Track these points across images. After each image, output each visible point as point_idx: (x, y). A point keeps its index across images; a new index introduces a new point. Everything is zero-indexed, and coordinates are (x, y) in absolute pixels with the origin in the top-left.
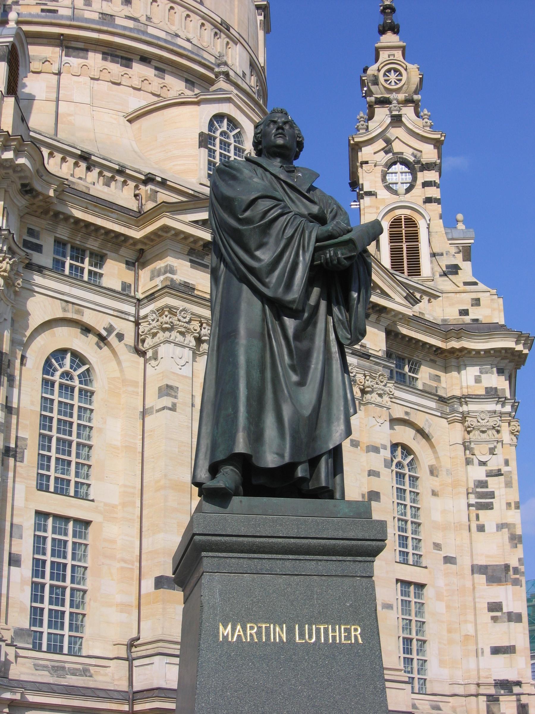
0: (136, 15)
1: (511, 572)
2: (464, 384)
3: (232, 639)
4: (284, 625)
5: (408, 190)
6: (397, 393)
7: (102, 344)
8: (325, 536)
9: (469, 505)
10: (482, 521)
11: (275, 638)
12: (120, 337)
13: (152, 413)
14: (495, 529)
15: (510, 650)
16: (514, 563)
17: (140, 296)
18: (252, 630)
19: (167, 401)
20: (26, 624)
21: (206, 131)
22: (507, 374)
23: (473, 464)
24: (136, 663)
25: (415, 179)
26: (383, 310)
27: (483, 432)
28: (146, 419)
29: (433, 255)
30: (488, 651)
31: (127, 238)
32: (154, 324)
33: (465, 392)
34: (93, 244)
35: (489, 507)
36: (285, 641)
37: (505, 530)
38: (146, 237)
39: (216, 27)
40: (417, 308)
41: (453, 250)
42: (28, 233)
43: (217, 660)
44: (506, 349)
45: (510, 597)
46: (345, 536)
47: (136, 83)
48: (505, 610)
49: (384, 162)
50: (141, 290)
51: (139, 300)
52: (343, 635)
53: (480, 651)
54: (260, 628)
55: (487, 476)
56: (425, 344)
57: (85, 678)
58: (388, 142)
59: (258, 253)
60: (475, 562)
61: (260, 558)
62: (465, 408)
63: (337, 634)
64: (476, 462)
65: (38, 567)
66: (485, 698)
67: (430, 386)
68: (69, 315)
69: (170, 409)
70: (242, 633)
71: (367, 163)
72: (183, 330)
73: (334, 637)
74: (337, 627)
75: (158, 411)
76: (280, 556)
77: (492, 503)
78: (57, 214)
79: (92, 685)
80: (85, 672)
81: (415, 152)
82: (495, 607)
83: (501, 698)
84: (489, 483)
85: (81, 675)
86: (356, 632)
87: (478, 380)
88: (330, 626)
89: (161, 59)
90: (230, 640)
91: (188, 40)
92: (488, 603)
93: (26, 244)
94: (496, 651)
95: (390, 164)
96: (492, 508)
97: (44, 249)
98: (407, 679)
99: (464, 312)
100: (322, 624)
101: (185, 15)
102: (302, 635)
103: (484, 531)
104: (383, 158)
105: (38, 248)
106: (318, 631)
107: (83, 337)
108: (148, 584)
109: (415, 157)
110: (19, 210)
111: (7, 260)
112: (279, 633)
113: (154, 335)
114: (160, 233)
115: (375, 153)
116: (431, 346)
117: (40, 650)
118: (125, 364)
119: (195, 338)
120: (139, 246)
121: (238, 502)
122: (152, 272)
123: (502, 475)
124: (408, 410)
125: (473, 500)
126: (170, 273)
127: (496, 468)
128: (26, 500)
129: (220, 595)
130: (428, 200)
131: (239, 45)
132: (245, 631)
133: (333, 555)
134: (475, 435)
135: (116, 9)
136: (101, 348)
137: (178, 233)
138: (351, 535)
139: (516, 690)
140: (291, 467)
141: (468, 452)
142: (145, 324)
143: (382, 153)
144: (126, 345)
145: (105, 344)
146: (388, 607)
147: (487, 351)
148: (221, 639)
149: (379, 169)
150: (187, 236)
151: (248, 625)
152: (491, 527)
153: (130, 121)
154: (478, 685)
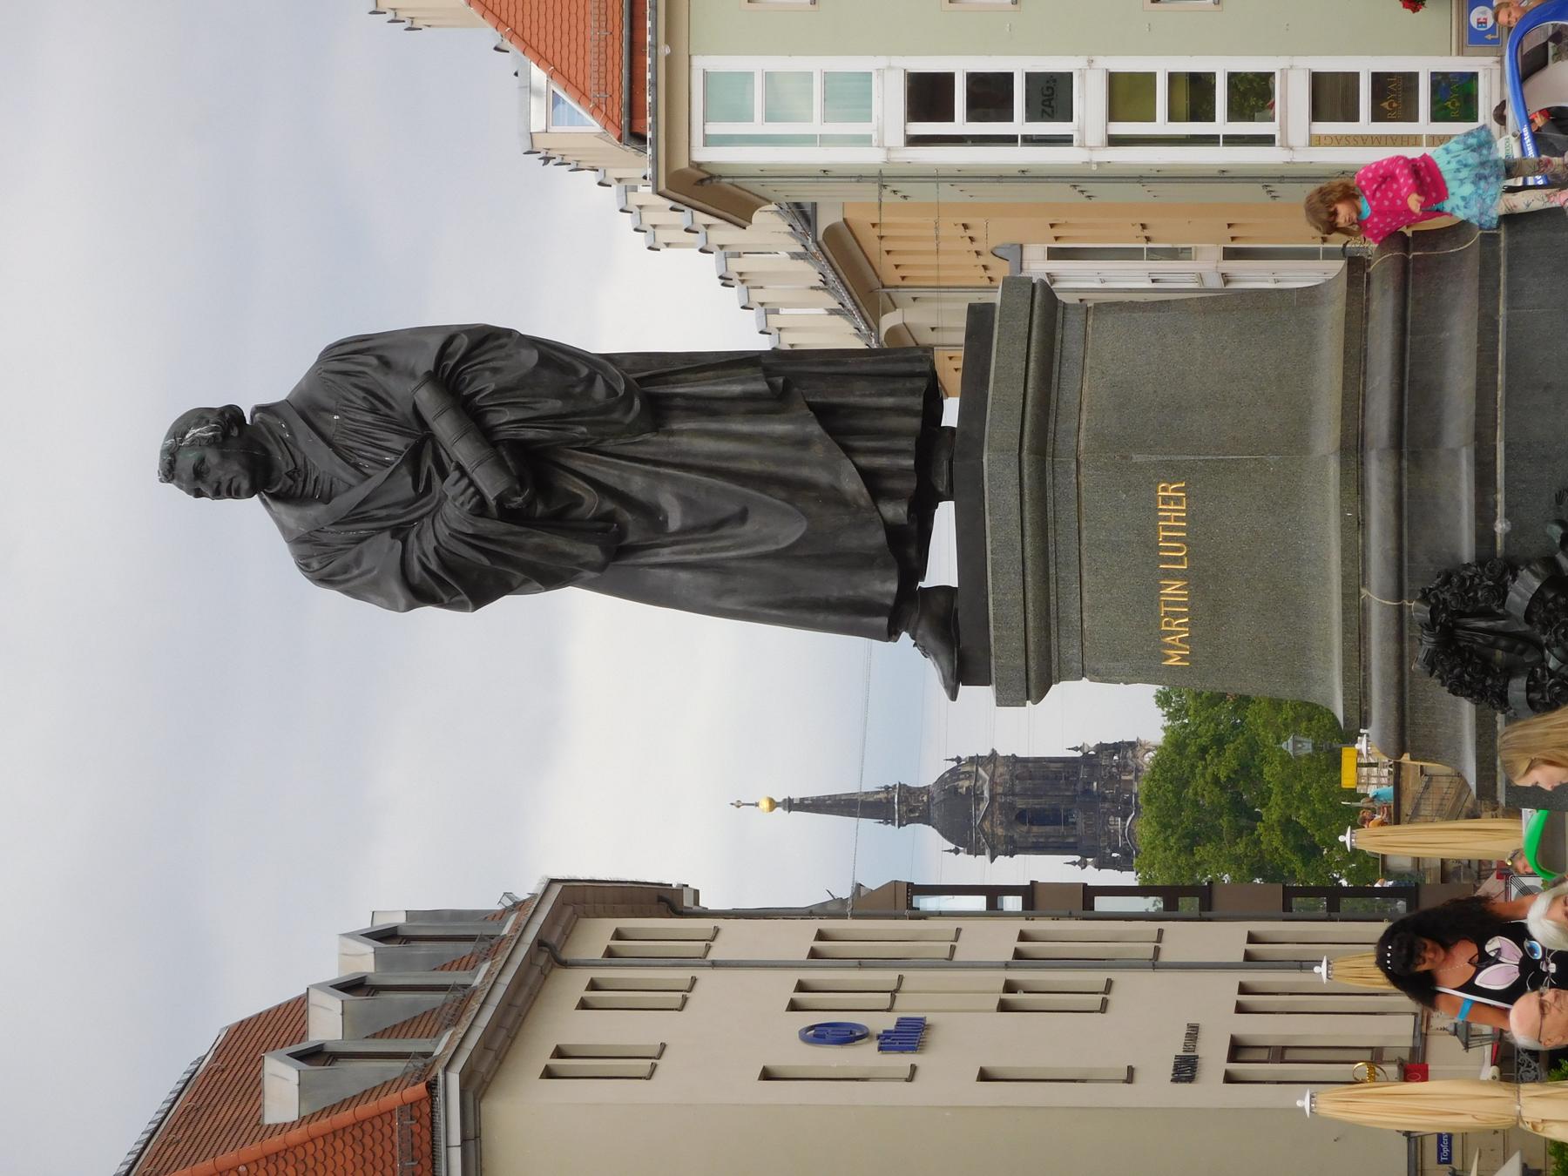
46: (1016, 511)
73: (1177, 519)
76: (1052, 586)
100: (1157, 533)
106: (1166, 539)
112: (1173, 590)
132: (1172, 633)
138: (1015, 501)
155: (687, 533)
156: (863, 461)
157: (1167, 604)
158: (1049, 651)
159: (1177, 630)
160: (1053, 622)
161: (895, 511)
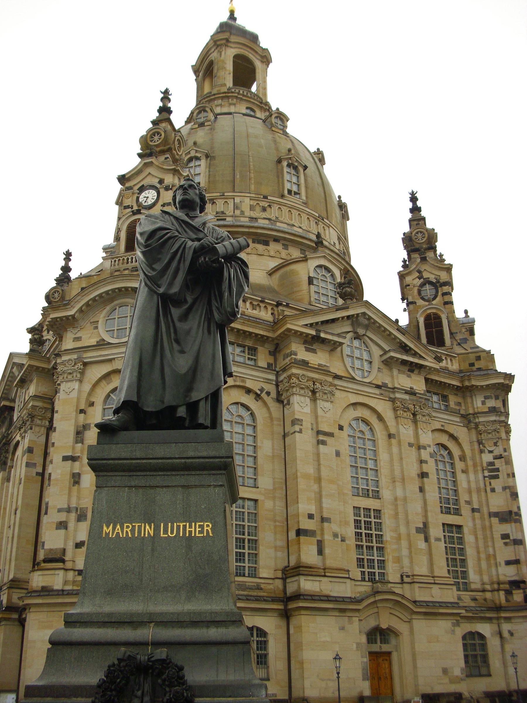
0: (269, 217)
1: (513, 515)
2: (475, 406)
3: (112, 535)
4: (153, 524)
5: (434, 299)
6: (434, 414)
7: (258, 399)
8: (185, 456)
9: (485, 477)
10: (493, 485)
11: (144, 534)
12: (268, 394)
13: (288, 435)
14: (501, 490)
15: (517, 562)
16: (515, 510)
17: (277, 369)
18: (127, 529)
19: (297, 428)
21: (312, 275)
22: (501, 399)
23: (485, 453)
24: (288, 580)
25: (437, 292)
26: (420, 367)
27: (489, 433)
29: (451, 334)
30: (503, 563)
31: (268, 337)
32: (287, 385)
33: (476, 410)
34: (249, 343)
35: (497, 477)
36: (152, 535)
37: (508, 490)
38: (279, 336)
39: (316, 219)
40: (443, 364)
41: (464, 330)
43: (100, 551)
44: (499, 384)
45: (514, 530)
47: (272, 253)
48: (511, 538)
49: (418, 285)
50: (278, 367)
51: (278, 372)
52: (198, 529)
53: (498, 563)
54: (134, 527)
55: (494, 459)
56: (450, 384)
58: (419, 272)
59: (154, 266)
60: (491, 511)
61: (138, 475)
62: (477, 420)
63: (193, 530)
64: (486, 451)
66: (503, 592)
67: (455, 409)
69: (299, 432)
70: (120, 531)
71: (409, 285)
72: (303, 386)
73: (190, 532)
74: (193, 524)
75: (292, 434)
77: (498, 475)
81: (436, 277)
82: (505, 536)
83: (514, 592)
84: (496, 463)
86: (208, 527)
87: (483, 403)
88: (188, 524)
89: (285, 239)
90: (110, 536)
91: (300, 227)
92: (501, 535)
94: (508, 563)
95: (422, 285)
96: (499, 478)
98: (453, 583)
99: (472, 365)
100: (182, 522)
101: (297, 214)
102: (165, 532)
103: (495, 492)
104: (418, 282)
106: (178, 527)
108: (292, 535)
109: (436, 279)
112: (148, 530)
113: (287, 390)
114: (286, 333)
115: (413, 280)
116: (454, 385)
118: (272, 409)
119: (311, 390)
120: (276, 341)
121: (124, 435)
122: (284, 355)
123: (503, 458)
124: (443, 424)
125: (486, 474)
127: (498, 454)
129: (106, 503)
130: (446, 303)
131: (331, 228)
133: (193, 471)
134: (484, 436)
135: (258, 215)
136: (257, 401)
137: (296, 332)
138: (205, 454)
139: (522, 585)
140: (173, 409)
141: (481, 446)
142: (282, 385)
143: (418, 280)
144: (272, 398)
145: (260, 399)
146: (438, 539)
147: (487, 386)
148: (104, 536)
149: (416, 288)
150: (302, 333)
151: (125, 525)
152: (499, 489)
153: (270, 275)
154: (499, 584)
156: (202, 404)
157: (140, 527)
158: (116, 471)
159: (126, 530)
160: (131, 474)
161: (182, 412)
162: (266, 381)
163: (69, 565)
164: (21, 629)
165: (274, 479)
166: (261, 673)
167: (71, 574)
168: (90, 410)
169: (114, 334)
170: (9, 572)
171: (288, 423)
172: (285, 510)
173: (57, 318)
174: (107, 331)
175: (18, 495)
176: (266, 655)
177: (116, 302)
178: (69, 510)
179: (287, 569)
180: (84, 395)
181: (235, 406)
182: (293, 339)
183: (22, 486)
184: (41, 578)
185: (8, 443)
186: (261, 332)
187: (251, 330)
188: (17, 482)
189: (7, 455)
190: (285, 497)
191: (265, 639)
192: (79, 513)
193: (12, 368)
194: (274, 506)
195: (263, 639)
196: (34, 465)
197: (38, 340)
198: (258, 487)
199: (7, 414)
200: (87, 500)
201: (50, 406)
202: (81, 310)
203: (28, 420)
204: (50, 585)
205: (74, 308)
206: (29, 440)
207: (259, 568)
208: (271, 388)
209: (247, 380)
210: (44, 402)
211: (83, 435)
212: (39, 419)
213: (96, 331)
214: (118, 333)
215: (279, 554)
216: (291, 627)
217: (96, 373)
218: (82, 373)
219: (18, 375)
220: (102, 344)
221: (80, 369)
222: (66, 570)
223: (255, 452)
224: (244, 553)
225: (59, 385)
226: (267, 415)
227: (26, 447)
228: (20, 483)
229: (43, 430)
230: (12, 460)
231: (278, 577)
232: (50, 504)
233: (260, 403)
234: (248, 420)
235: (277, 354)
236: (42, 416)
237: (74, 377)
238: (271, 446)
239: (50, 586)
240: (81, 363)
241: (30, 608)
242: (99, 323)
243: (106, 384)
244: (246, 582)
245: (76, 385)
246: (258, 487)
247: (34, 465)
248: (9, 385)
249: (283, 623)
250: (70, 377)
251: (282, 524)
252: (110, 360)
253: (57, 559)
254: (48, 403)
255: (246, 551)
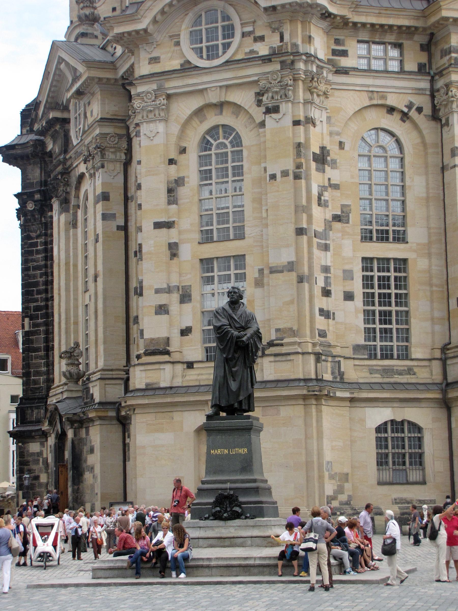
7: (405, 119)
12: (420, 110)
13: (447, 170)
20: (361, 341)
28: (446, 173)
31: (416, 28)
32: (445, 97)
34: (390, 38)
42: (335, 42)
50: (434, 67)
57: (408, 376)
65: (369, 299)
68: (375, 102)
78: (355, 24)
79: (414, 381)
80: (410, 371)
85: (407, 374)
86: (246, 450)
93: (334, 53)
97: (350, 53)
105: (344, 53)
107: (389, 116)
110: (323, 29)
111: (315, 79)
112: (226, 451)
113: (446, 106)
114: (441, 22)
117: (375, 358)
118: (425, 132)
120: (429, 32)
126: (454, 53)
128: (354, 251)
136: (404, 121)
145: (408, 118)
155: (231, 372)
159: (219, 452)
161: (236, 405)
162: (417, 92)
163: (176, 357)
164: (120, 429)
165: (429, 228)
166: (415, 476)
167: (180, 368)
168: (182, 159)
169: (201, 52)
170: (97, 357)
171: (447, 152)
172: (445, 270)
173: (123, 33)
174: (193, 49)
175: (96, 256)
176: (421, 456)
177: (200, 6)
178: (169, 290)
179: (448, 347)
180: (173, 140)
181: (373, 132)
182: (452, 28)
183: (100, 245)
184: (144, 372)
185: (67, 172)
186: (406, 22)
187: (391, 21)
188: (91, 238)
189: (68, 190)
190: (444, 253)
191: (419, 435)
192: (181, 293)
193: (59, 63)
194: (430, 266)
195: (416, 435)
196: (113, 216)
197: (90, 17)
198: (407, 242)
199: (60, 128)
200: (189, 276)
201: (124, 132)
202: (155, 21)
203: (97, 153)
204: (155, 381)
205: (145, 17)
206: (103, 184)
207: (411, 347)
208: (423, 101)
209: (388, 94)
210: (116, 127)
211: (177, 192)
212: (112, 152)
213: (177, 48)
214: (208, 51)
215: (437, 328)
216: (453, 419)
217: (184, 108)
218: (167, 109)
219: (72, 84)
220: (187, 68)
221: (163, 105)
222: (173, 363)
223: (403, 194)
224: (391, 329)
225: (137, 125)
226: (419, 140)
227: (99, 191)
228: (97, 241)
229: (119, 167)
230: (77, 197)
231: (436, 357)
232: (144, 284)
233: (407, 124)
234: (393, 150)
235: (433, 48)
236: (115, 148)
237: (157, 115)
238: (424, 184)
239: (156, 384)
240: (164, 97)
241: (134, 410)
242: (182, 37)
243: (198, 123)
244: (394, 366)
245: (161, 127)
246: (407, 242)
247: (113, 216)
248: (55, 86)
249: (443, 414)
250: (151, 116)
251: (441, 289)
252: (201, 91)
253: (160, 350)
254: (122, 127)
255: (394, 326)
